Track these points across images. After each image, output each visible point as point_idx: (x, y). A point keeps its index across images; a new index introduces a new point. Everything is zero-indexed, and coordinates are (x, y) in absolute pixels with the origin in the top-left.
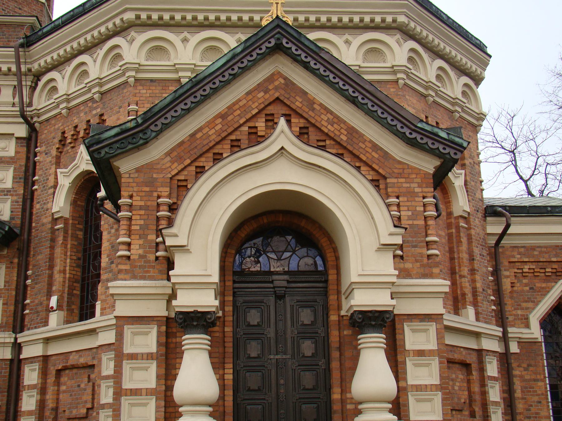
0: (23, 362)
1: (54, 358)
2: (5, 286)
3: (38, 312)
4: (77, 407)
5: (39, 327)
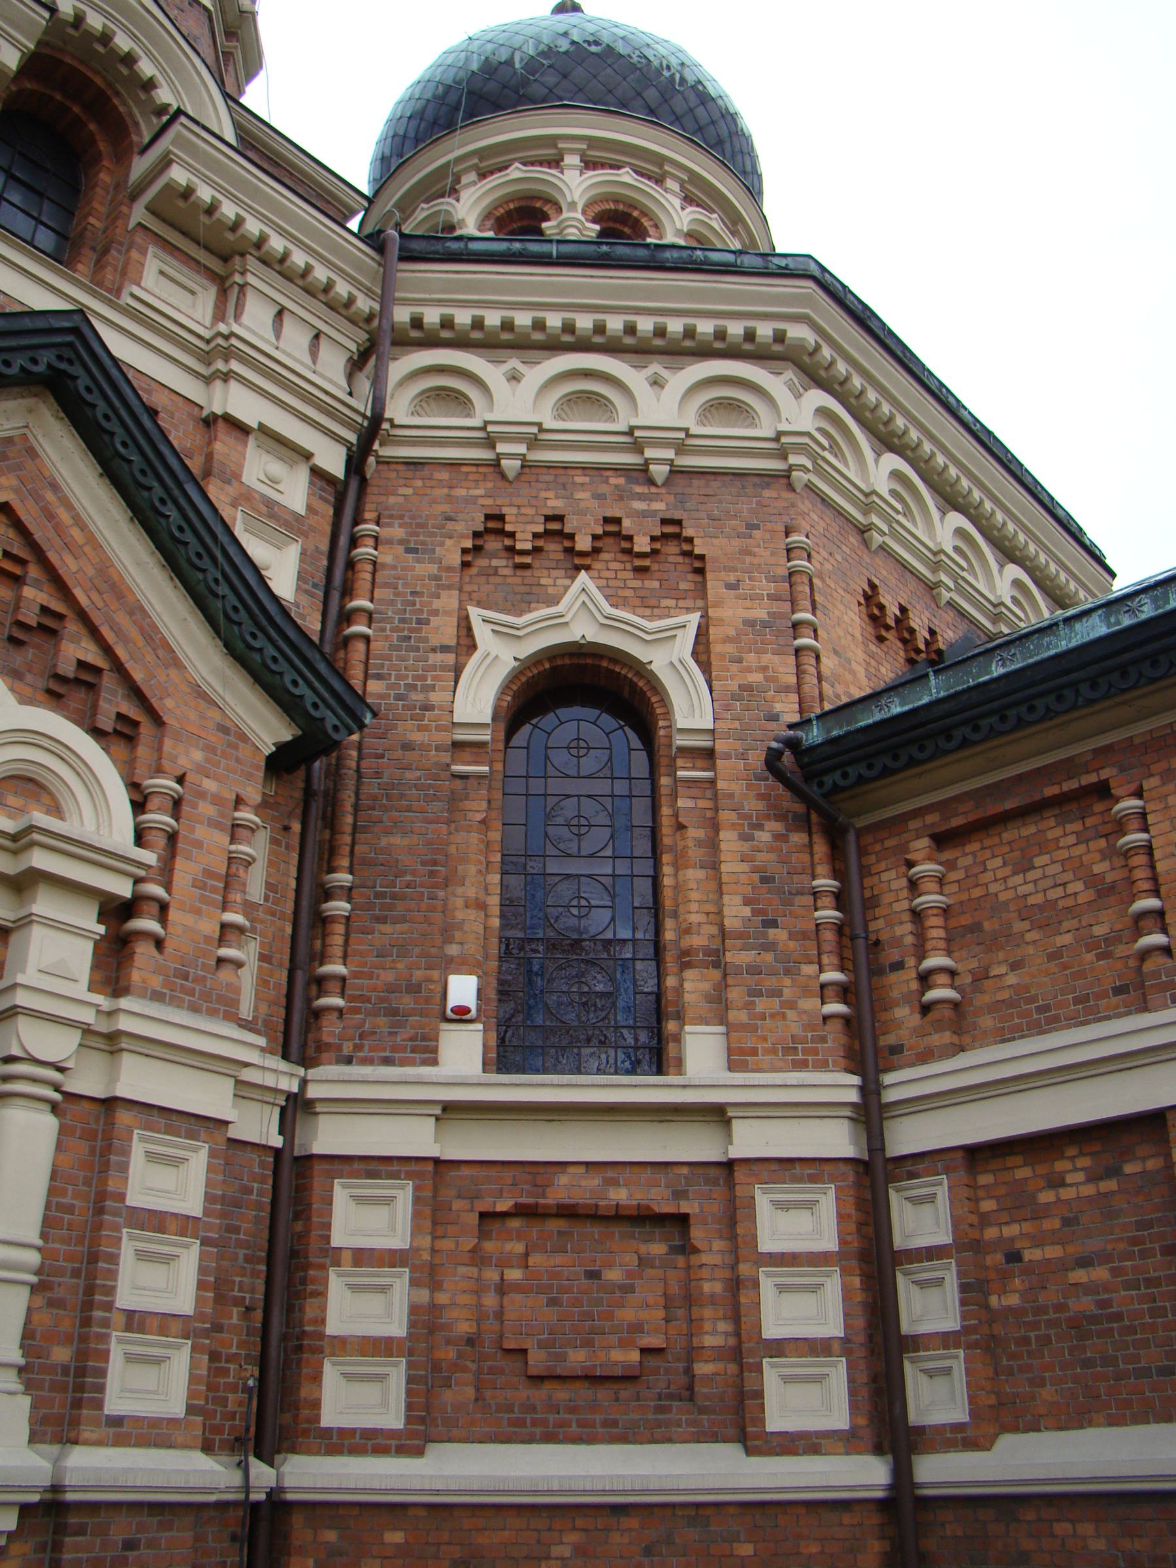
0: (318, 1167)
1: (466, 1171)
2: (266, 898)
3: (394, 1012)
4: (588, 1343)
5: (403, 1063)
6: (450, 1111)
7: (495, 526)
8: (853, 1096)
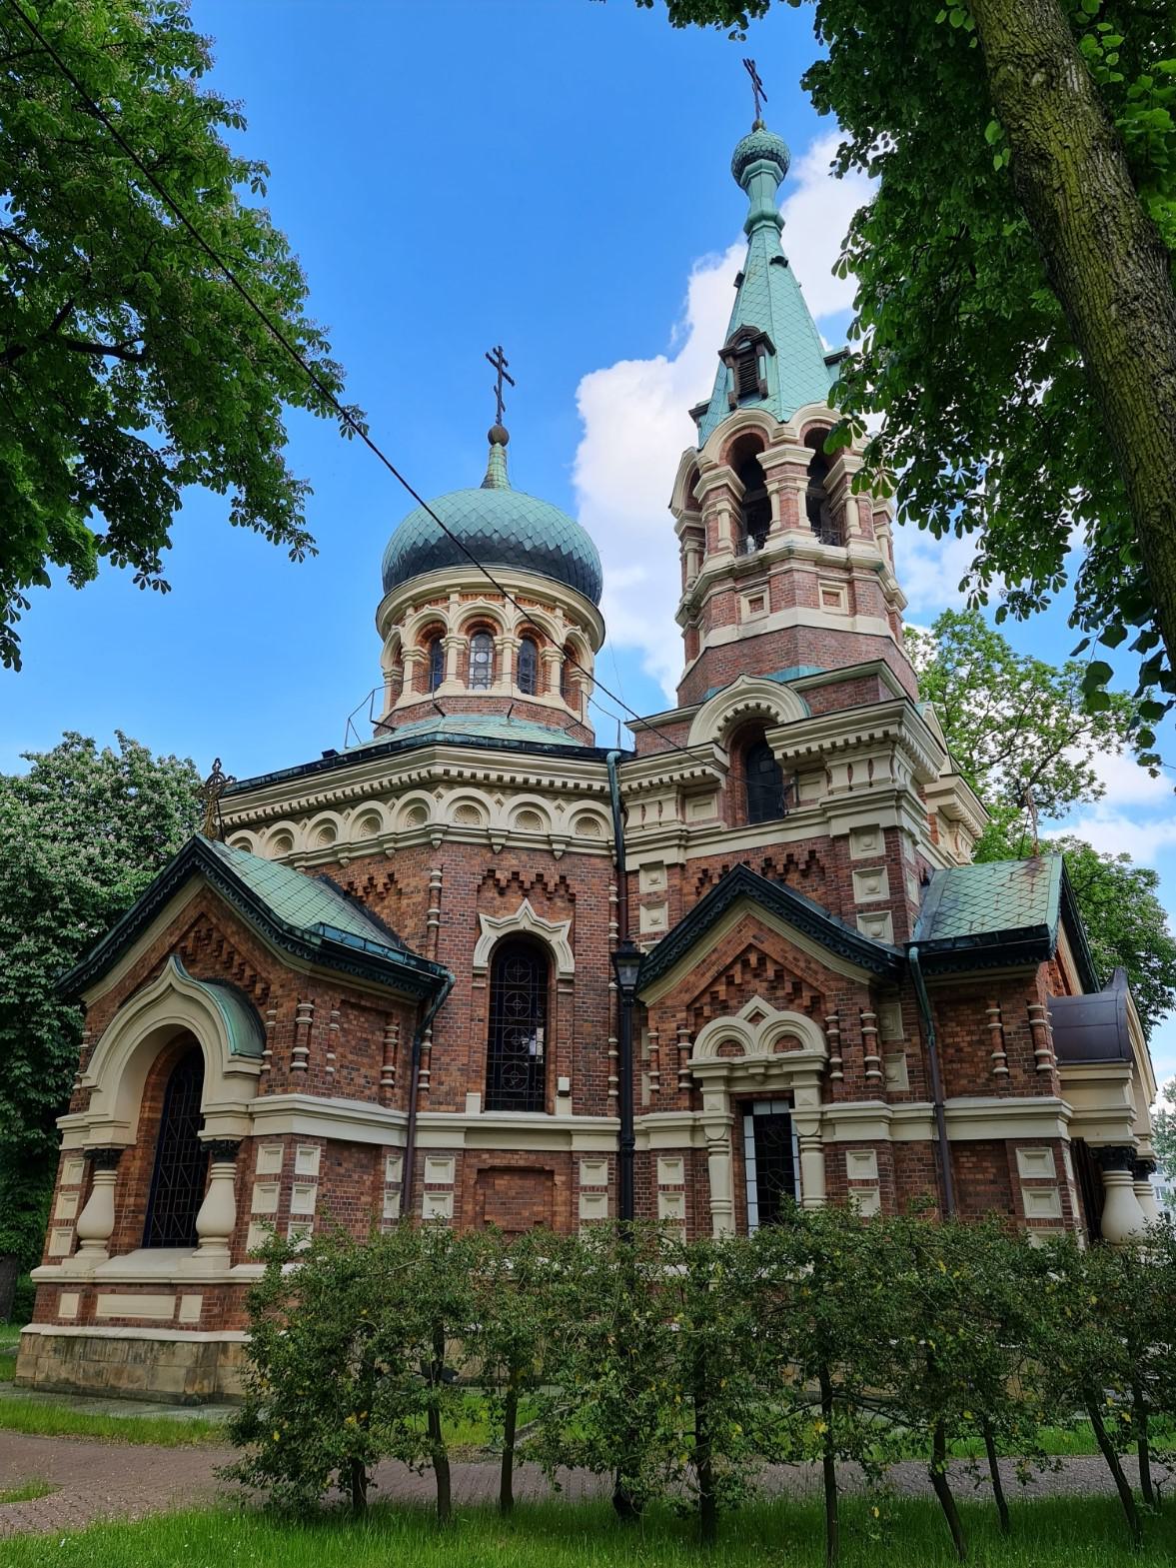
6: (470, 1132)
7: (491, 872)
8: (618, 1128)
